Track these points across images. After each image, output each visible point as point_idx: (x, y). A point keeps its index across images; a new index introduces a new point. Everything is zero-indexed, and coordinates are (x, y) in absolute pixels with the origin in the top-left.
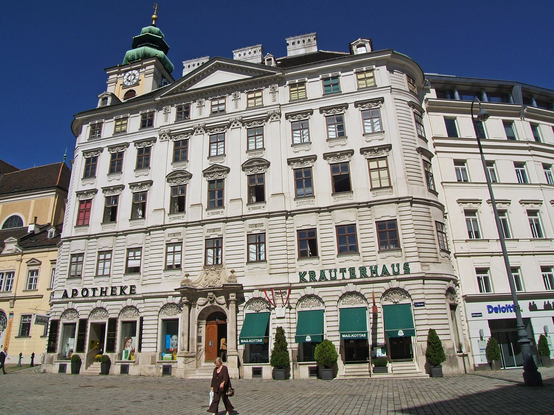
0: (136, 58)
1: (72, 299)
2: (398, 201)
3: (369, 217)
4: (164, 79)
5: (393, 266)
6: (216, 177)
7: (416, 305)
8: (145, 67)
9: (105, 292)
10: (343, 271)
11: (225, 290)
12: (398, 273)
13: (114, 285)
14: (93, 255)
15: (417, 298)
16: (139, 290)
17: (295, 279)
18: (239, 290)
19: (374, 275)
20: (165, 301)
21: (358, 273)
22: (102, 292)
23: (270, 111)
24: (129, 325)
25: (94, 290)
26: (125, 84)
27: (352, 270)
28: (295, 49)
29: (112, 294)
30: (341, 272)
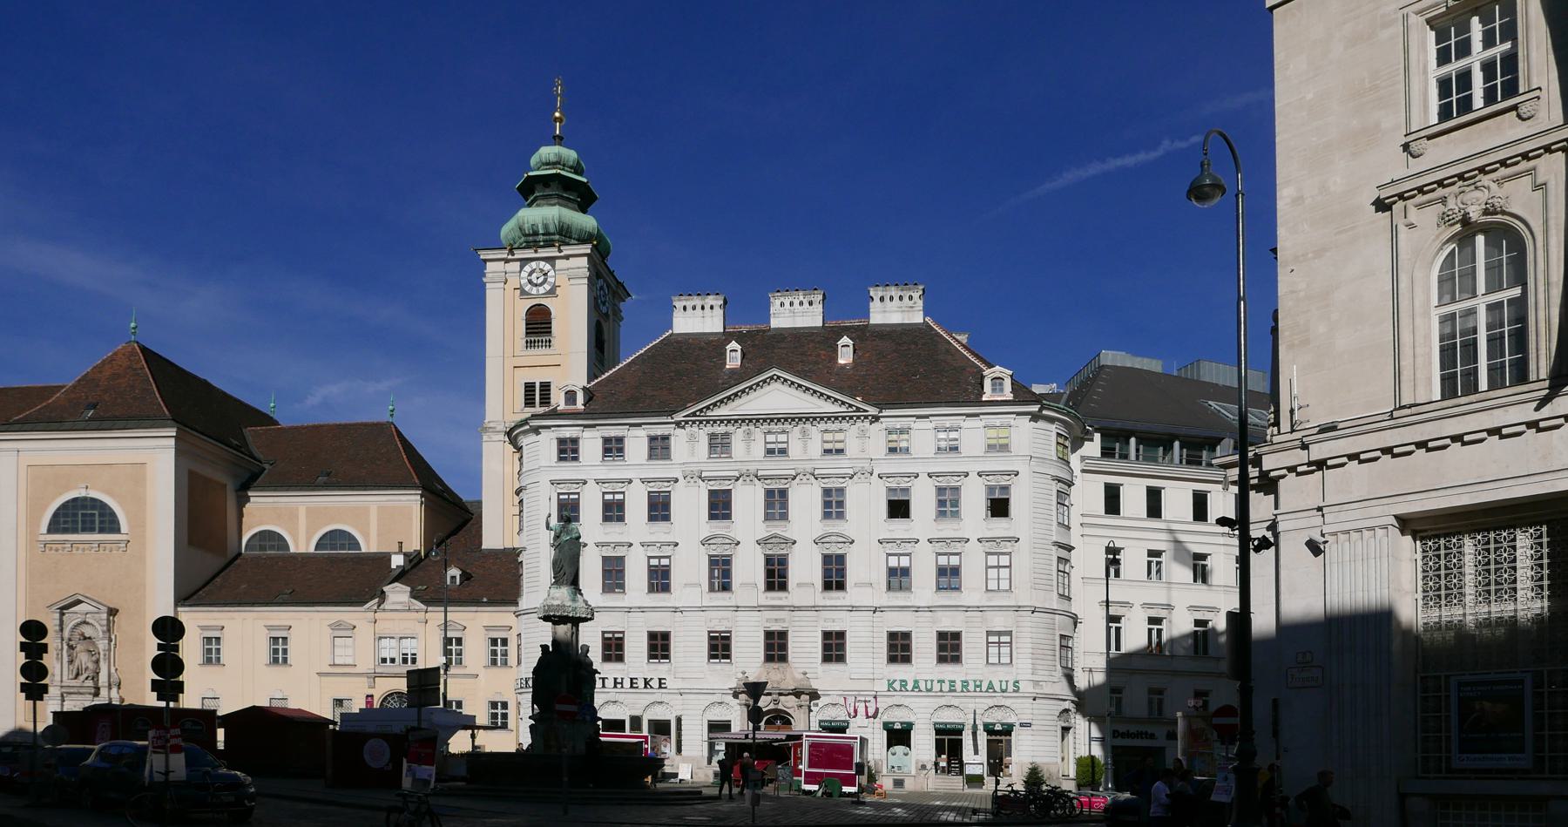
0: (541, 232)
7: (1022, 725)
8: (567, 257)
9: (622, 683)
10: (941, 682)
11: (797, 693)
17: (882, 687)
18: (814, 695)
19: (978, 689)
22: (616, 683)
26: (527, 289)
27: (952, 682)
29: (632, 687)
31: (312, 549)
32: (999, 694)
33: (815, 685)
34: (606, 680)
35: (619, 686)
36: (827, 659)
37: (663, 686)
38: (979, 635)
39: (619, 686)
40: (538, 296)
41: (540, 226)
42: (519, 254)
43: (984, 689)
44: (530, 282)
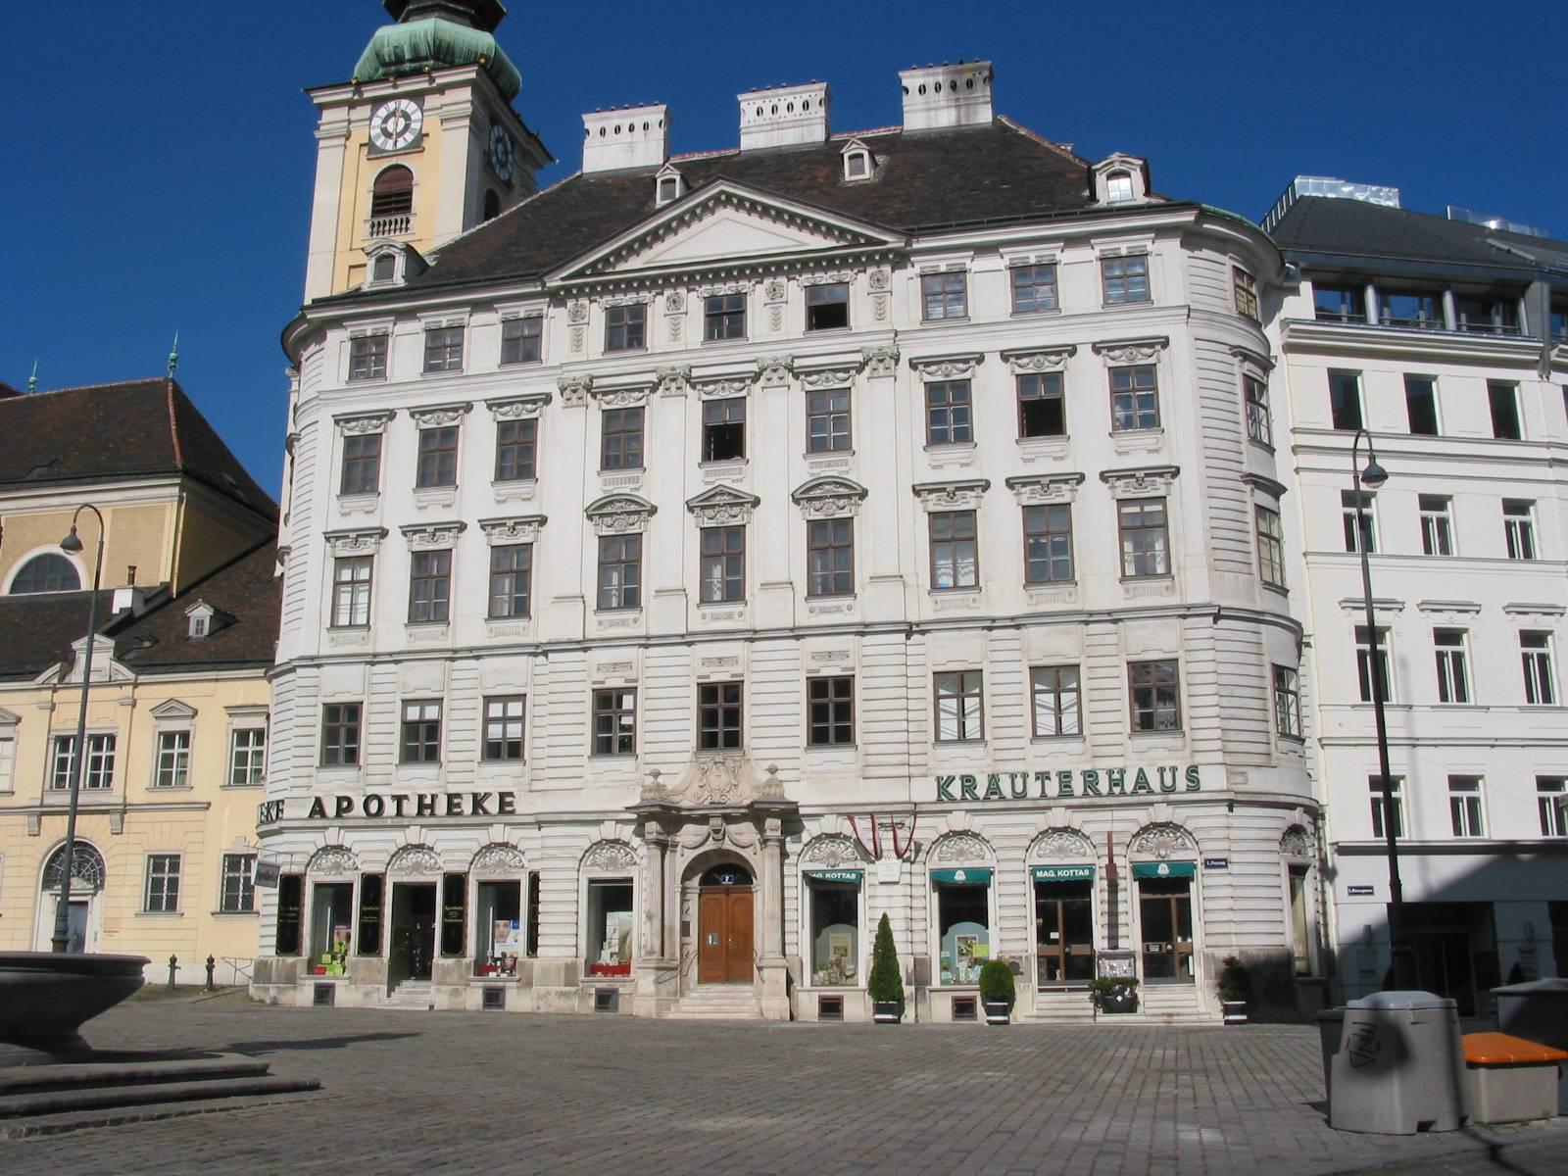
0: (407, 56)
2: (1186, 612)
3: (1113, 650)
4: (495, 129)
5: (1162, 770)
6: (724, 519)
8: (441, 90)
9: (432, 806)
10: (1042, 777)
11: (756, 814)
12: (1172, 790)
13: (452, 790)
14: (389, 707)
15: (1214, 848)
16: (522, 805)
17: (925, 791)
19: (1117, 790)
20: (595, 833)
21: (1078, 784)
22: (421, 806)
23: (874, 344)
24: (491, 889)
26: (378, 143)
27: (1065, 777)
28: (929, 110)
29: (450, 813)
30: (1037, 779)
32: (1159, 798)
33: (791, 793)
34: (405, 801)
35: (428, 812)
36: (818, 737)
37: (508, 809)
38: (1114, 672)
39: (428, 812)
40: (397, 153)
41: (406, 49)
42: (370, 92)
43: (1129, 786)
44: (387, 134)
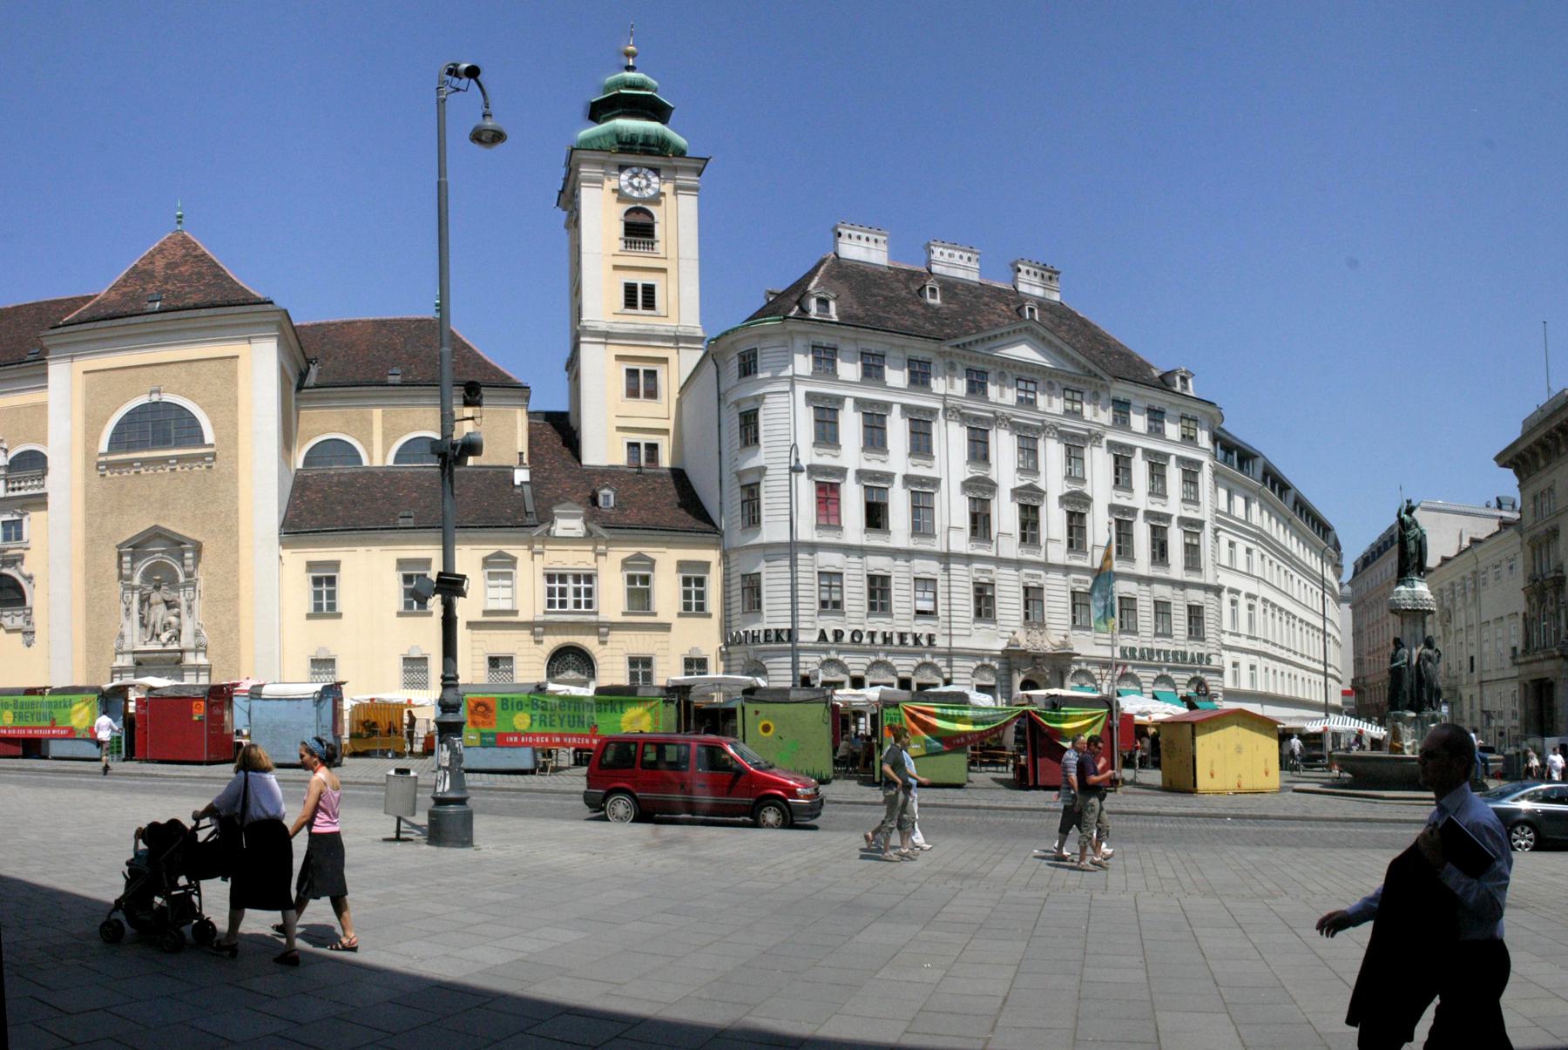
1: (835, 646)
9: (891, 638)
16: (941, 642)
25: (872, 634)
31: (390, 462)
40: (644, 200)
44: (631, 185)
